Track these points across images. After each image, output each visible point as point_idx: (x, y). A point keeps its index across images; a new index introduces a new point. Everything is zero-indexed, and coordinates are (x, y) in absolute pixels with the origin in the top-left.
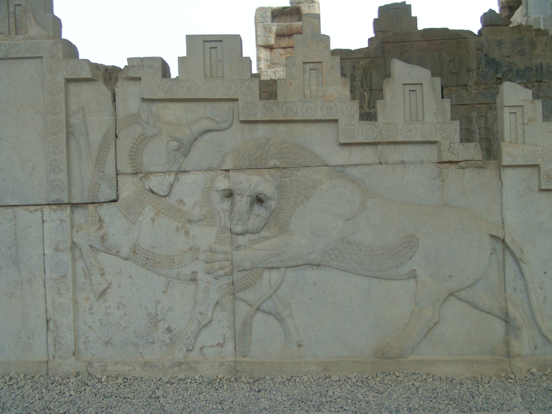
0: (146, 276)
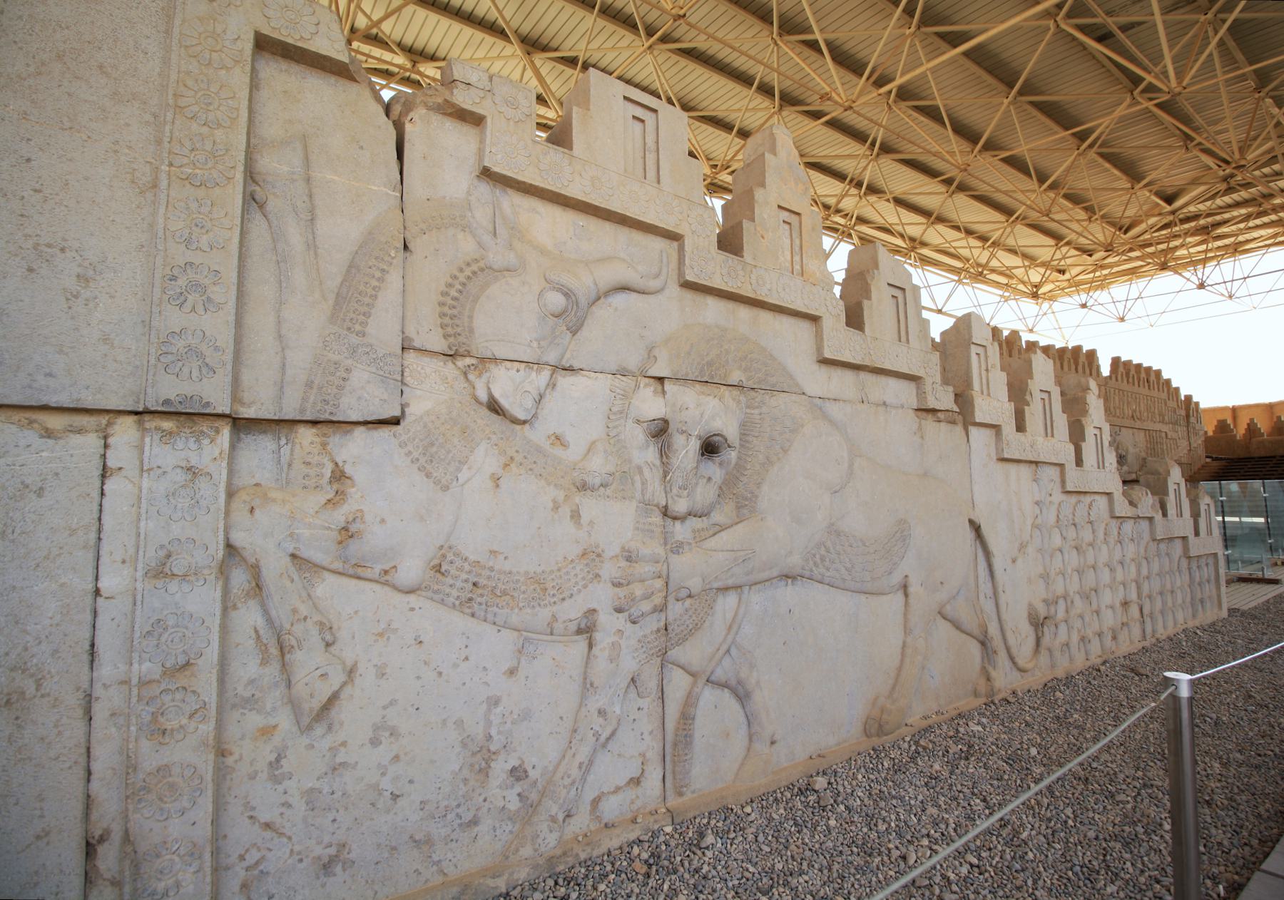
0: (463, 634)
